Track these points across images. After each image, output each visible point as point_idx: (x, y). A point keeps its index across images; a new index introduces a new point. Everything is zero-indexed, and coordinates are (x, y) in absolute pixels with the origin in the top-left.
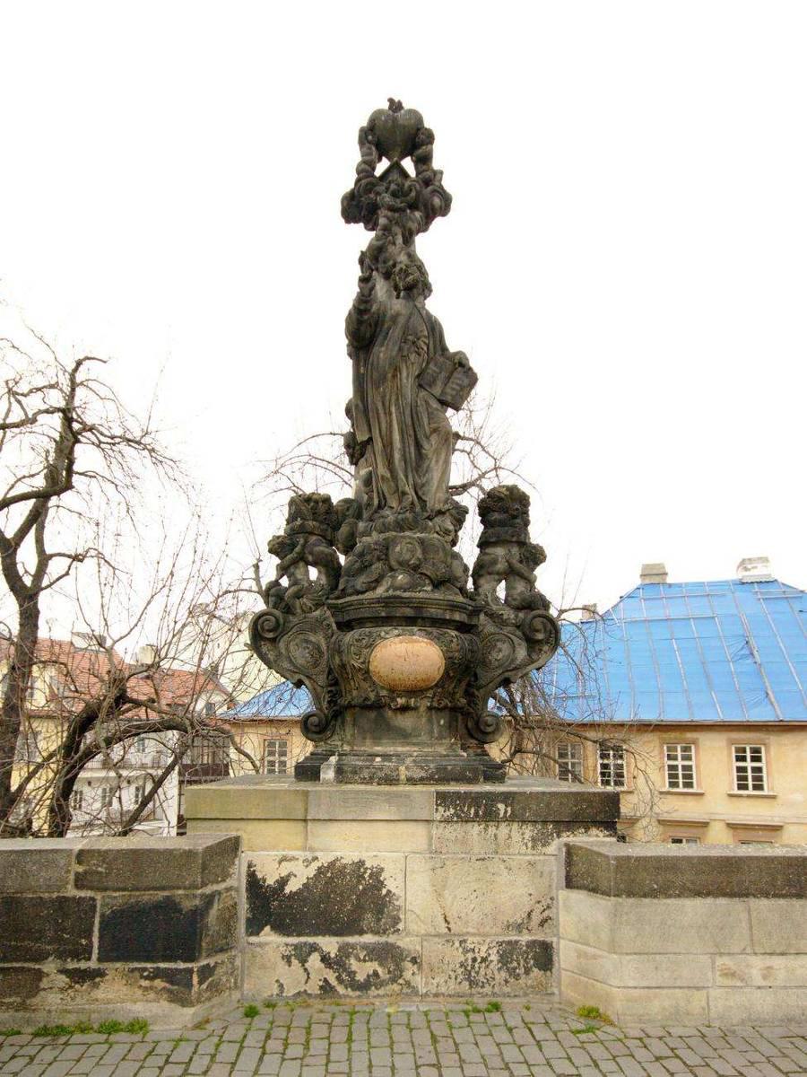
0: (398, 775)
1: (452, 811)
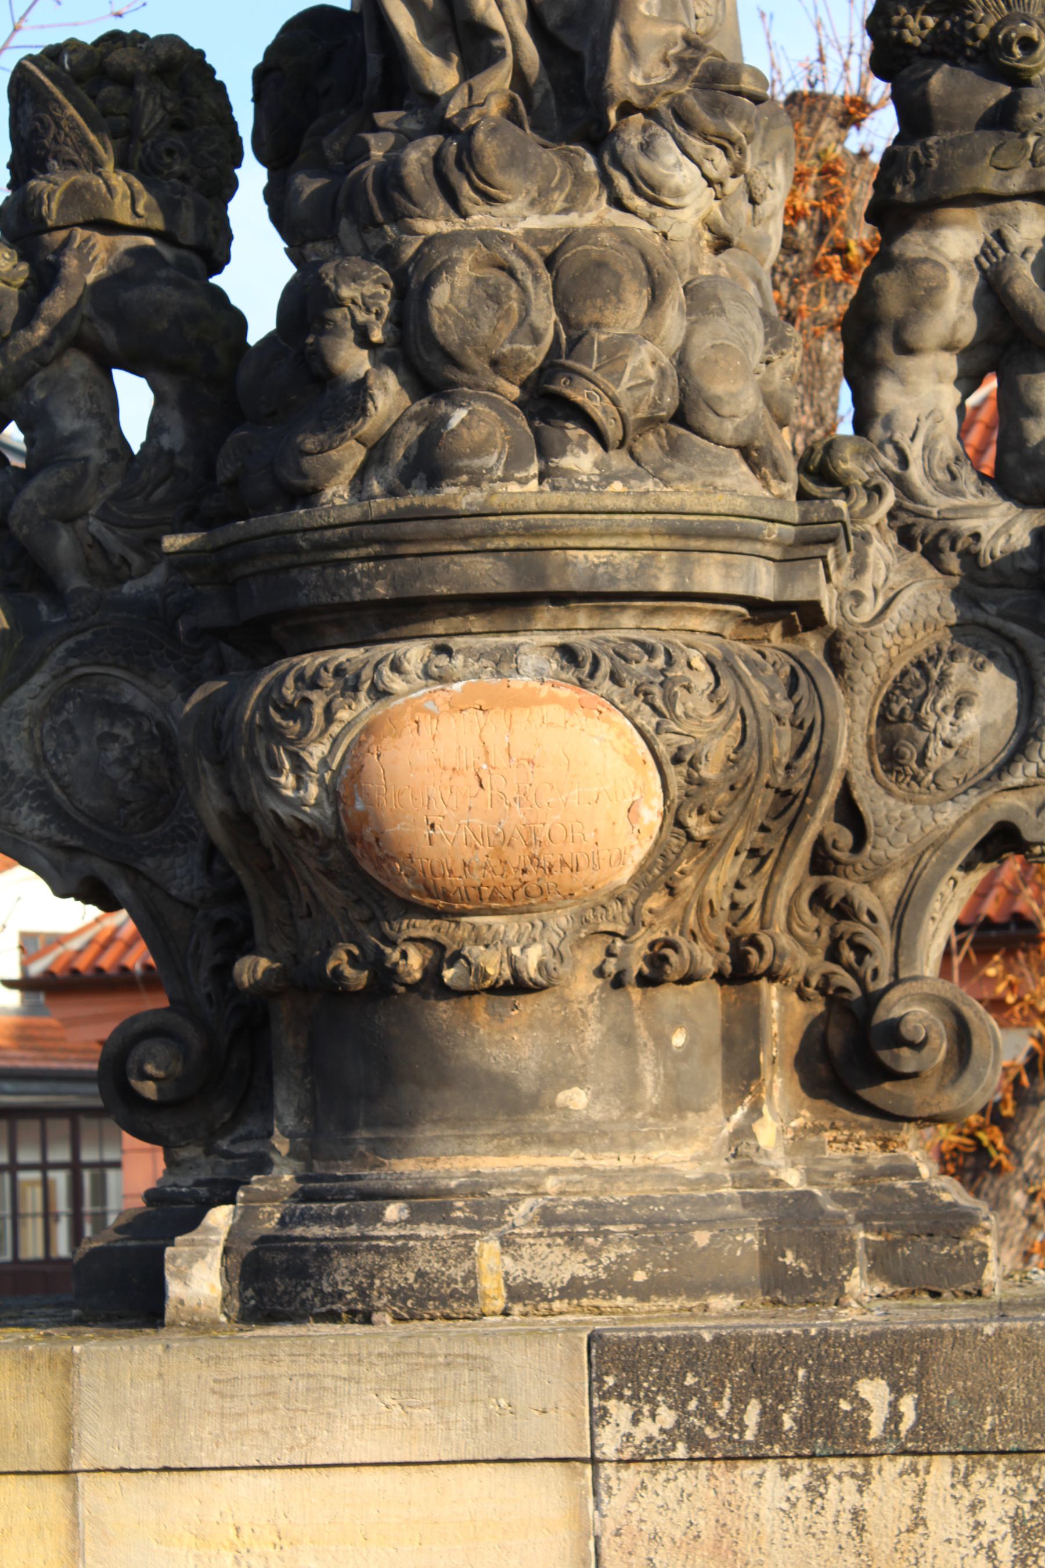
0: (472, 1275)
1: (667, 1417)
